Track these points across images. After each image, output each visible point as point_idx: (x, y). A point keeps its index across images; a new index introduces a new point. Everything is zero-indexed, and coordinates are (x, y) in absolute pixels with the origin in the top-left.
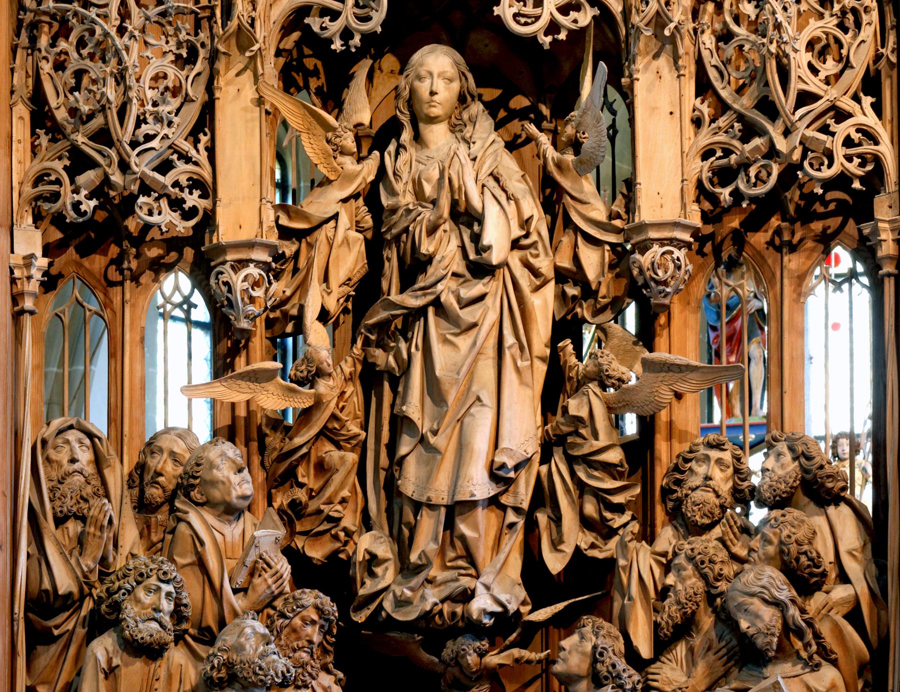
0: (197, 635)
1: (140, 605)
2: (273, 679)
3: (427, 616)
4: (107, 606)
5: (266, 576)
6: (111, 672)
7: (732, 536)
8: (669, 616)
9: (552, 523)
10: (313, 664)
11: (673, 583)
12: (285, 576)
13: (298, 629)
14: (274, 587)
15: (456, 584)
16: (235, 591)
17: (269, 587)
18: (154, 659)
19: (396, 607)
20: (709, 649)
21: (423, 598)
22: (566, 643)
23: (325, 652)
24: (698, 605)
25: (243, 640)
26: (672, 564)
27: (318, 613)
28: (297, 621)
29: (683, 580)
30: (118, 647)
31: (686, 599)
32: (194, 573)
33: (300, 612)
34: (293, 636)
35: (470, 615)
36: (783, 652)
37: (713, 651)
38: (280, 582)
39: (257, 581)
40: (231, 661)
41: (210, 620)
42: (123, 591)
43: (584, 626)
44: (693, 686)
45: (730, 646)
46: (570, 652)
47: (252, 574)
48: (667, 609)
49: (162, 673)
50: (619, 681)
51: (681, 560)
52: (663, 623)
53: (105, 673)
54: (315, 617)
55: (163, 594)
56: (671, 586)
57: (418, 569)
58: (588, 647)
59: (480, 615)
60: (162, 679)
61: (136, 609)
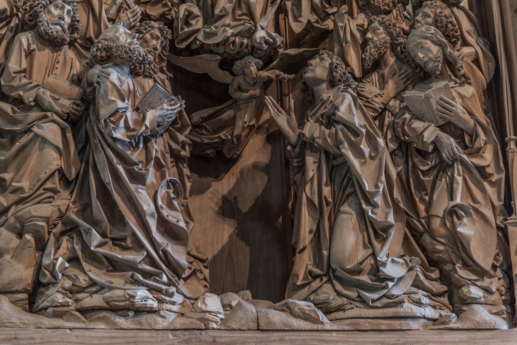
0: (82, 44)
1: (51, 15)
2: (137, 58)
3: (226, 41)
4: (29, 16)
5: (128, 12)
6: (29, 54)
7: (400, 19)
8: (370, 54)
9: (294, 6)
10: (155, 65)
11: (371, 38)
12: (139, 14)
13: (148, 40)
14: (131, 20)
15: (242, 27)
16: (110, 20)
17: (129, 19)
18: (57, 51)
19: (206, 38)
20: (394, 75)
21: (225, 31)
22: (313, 62)
23: (162, 60)
24: (387, 49)
25: (118, 34)
26: (369, 28)
27: (161, 33)
28: (148, 36)
29: (377, 35)
30: (35, 39)
31: (380, 45)
32: (83, 7)
33: (150, 30)
34: (145, 44)
35: (256, 41)
36: (442, 76)
37: (398, 75)
38: (135, 18)
39: (121, 14)
40: (109, 46)
41: (91, 33)
42: (41, 5)
43: (322, 54)
44: (388, 93)
45: (407, 72)
46: (315, 66)
47: (119, 11)
48: (369, 51)
49: (61, 59)
50: (347, 83)
51: (376, 24)
52: (367, 58)
53: (26, 52)
54: (159, 35)
55: (66, 10)
56: (370, 39)
57: (220, 17)
58: (327, 64)
59: (261, 40)
60: (60, 62)
61: (48, 17)
